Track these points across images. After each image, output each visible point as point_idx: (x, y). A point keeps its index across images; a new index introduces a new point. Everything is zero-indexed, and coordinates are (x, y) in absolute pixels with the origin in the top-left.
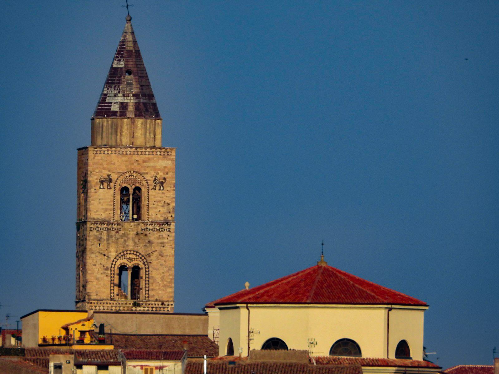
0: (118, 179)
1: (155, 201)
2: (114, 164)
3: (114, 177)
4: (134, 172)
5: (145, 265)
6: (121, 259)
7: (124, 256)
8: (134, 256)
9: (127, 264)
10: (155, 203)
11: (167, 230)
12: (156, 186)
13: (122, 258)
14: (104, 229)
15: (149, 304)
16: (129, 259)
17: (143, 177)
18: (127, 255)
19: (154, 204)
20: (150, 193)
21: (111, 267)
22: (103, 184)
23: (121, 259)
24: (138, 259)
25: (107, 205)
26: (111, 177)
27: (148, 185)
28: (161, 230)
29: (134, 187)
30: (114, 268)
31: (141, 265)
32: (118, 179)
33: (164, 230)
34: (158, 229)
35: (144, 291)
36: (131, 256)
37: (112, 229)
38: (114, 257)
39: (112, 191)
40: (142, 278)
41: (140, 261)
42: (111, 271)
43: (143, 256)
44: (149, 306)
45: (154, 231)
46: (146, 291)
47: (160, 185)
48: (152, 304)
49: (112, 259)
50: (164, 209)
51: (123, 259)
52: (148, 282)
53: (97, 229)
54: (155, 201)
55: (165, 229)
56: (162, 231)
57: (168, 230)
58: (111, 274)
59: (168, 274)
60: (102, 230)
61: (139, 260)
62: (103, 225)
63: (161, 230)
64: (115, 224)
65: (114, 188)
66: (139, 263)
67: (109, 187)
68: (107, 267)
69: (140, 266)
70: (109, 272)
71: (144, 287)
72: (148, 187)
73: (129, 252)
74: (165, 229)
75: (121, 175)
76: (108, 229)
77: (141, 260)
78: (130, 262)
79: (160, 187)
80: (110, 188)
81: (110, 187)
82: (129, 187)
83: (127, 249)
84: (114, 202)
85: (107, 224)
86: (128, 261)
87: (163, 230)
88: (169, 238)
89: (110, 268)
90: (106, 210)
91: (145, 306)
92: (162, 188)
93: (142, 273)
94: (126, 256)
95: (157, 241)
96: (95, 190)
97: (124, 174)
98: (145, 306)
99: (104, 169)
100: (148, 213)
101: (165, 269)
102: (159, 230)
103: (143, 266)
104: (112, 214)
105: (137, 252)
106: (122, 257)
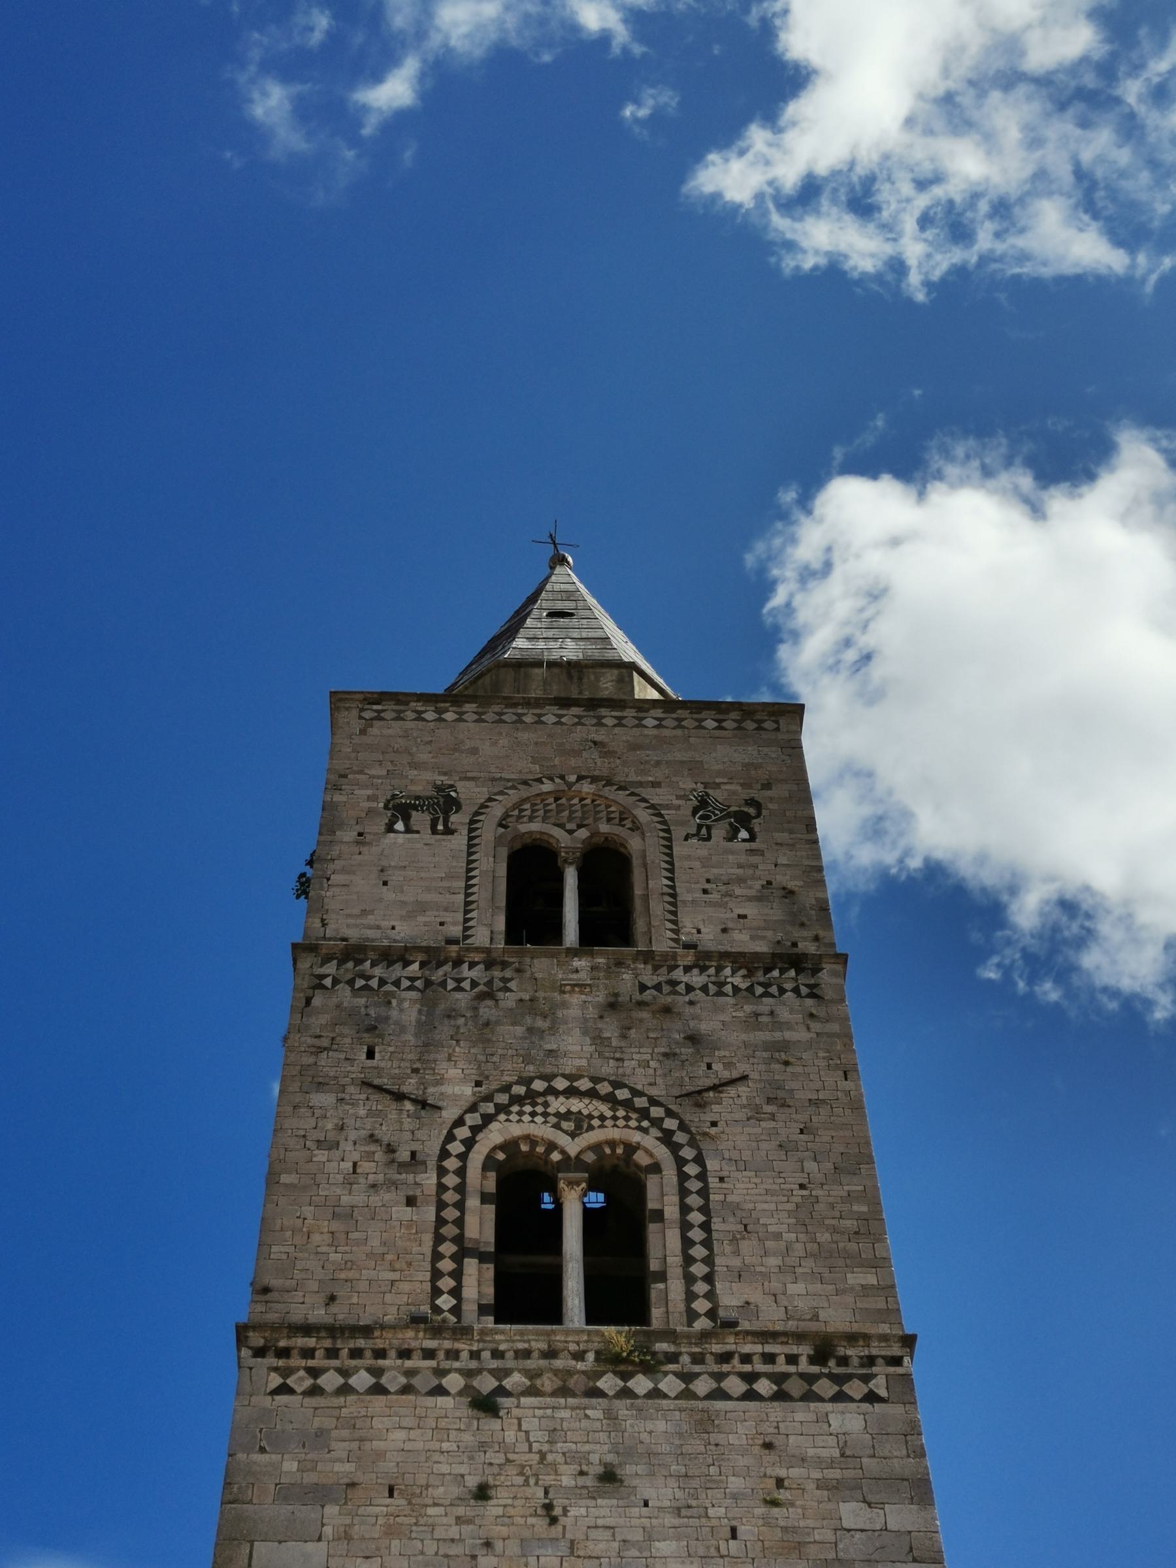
0: (490, 800)
1: (708, 881)
2: (474, 751)
3: (469, 793)
4: (580, 778)
5: (674, 1148)
6: (514, 1117)
7: (534, 1104)
8: (605, 1109)
9: (552, 1146)
10: (707, 886)
11: (796, 990)
12: (709, 828)
13: (521, 1113)
14: (406, 983)
15: (725, 1357)
16: (567, 1116)
17: (633, 794)
18: (551, 1099)
19: (705, 891)
20: (676, 850)
21: (444, 1154)
22: (406, 819)
23: (514, 1117)
24: (627, 1118)
25: (428, 890)
26: (453, 794)
27: (664, 822)
28: (759, 990)
29: (583, 834)
30: (463, 1157)
31: (650, 1145)
32: (490, 800)
33: (782, 991)
34: (743, 986)
35: (676, 1287)
36: (576, 1105)
37: (451, 984)
38: (465, 1105)
39: (459, 841)
40: (659, 1216)
41: (645, 1131)
42: (442, 1172)
43: (653, 1102)
44: (726, 1368)
45: (720, 993)
46: (690, 1279)
47: (731, 824)
48: (746, 1359)
49: (450, 1114)
50: (766, 911)
51: (527, 1118)
52: (700, 1238)
53: (360, 983)
54: (708, 881)
55: (788, 986)
56: (766, 994)
57: (804, 990)
58: (442, 1188)
59: (839, 1192)
60: (389, 988)
61: (633, 1123)
62: (398, 966)
63: (759, 990)
64: (472, 965)
65: (471, 830)
66: (636, 1137)
67: (440, 827)
68: (413, 1154)
69: (641, 1159)
70: (429, 1179)
71: (675, 1261)
72: (668, 831)
73: (561, 1084)
74: (788, 986)
75: (513, 787)
76: (428, 983)
77: (645, 1124)
78: (573, 1135)
79: (736, 831)
80: (449, 831)
81: (445, 824)
82: (557, 833)
83: (548, 1070)
84: (469, 878)
85: (423, 965)
86: (557, 1126)
87: (774, 990)
88: (816, 1026)
89: (432, 1163)
90: (422, 908)
91: (697, 1369)
92: (744, 834)
93: (662, 1194)
94: (546, 1105)
95: (744, 1037)
96: (360, 834)
97: (525, 783)
98: (697, 1369)
99: (415, 765)
100: (675, 922)
101: (811, 1166)
102: (750, 989)
103: (662, 1153)
104: (455, 924)
105: (617, 1085)
106: (515, 1108)
